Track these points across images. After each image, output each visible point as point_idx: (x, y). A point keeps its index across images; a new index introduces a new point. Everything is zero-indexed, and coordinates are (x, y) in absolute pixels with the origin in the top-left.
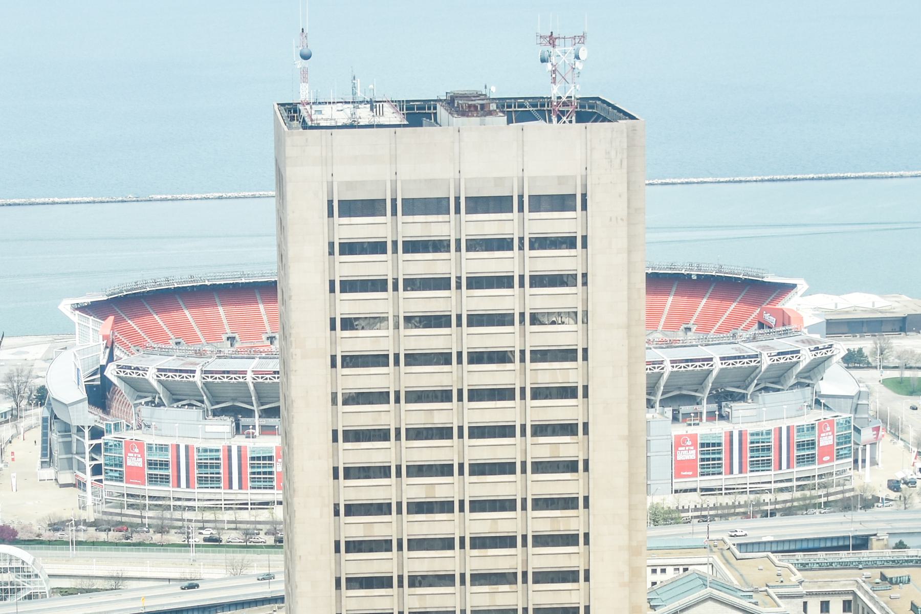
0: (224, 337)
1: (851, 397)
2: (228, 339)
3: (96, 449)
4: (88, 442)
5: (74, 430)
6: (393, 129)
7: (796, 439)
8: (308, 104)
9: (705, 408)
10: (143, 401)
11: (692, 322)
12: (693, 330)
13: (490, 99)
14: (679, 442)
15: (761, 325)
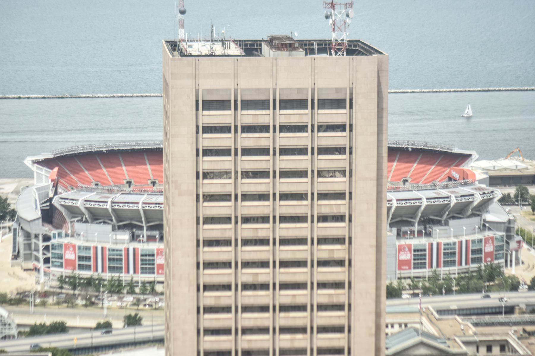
0: (125, 182)
1: (504, 223)
2: (127, 182)
3: (47, 248)
4: (41, 244)
5: (33, 236)
6: (236, 58)
7: (471, 247)
8: (184, 41)
9: (416, 228)
10: (76, 219)
11: (408, 176)
12: (409, 181)
13: (294, 41)
14: (401, 249)
15: (450, 179)
